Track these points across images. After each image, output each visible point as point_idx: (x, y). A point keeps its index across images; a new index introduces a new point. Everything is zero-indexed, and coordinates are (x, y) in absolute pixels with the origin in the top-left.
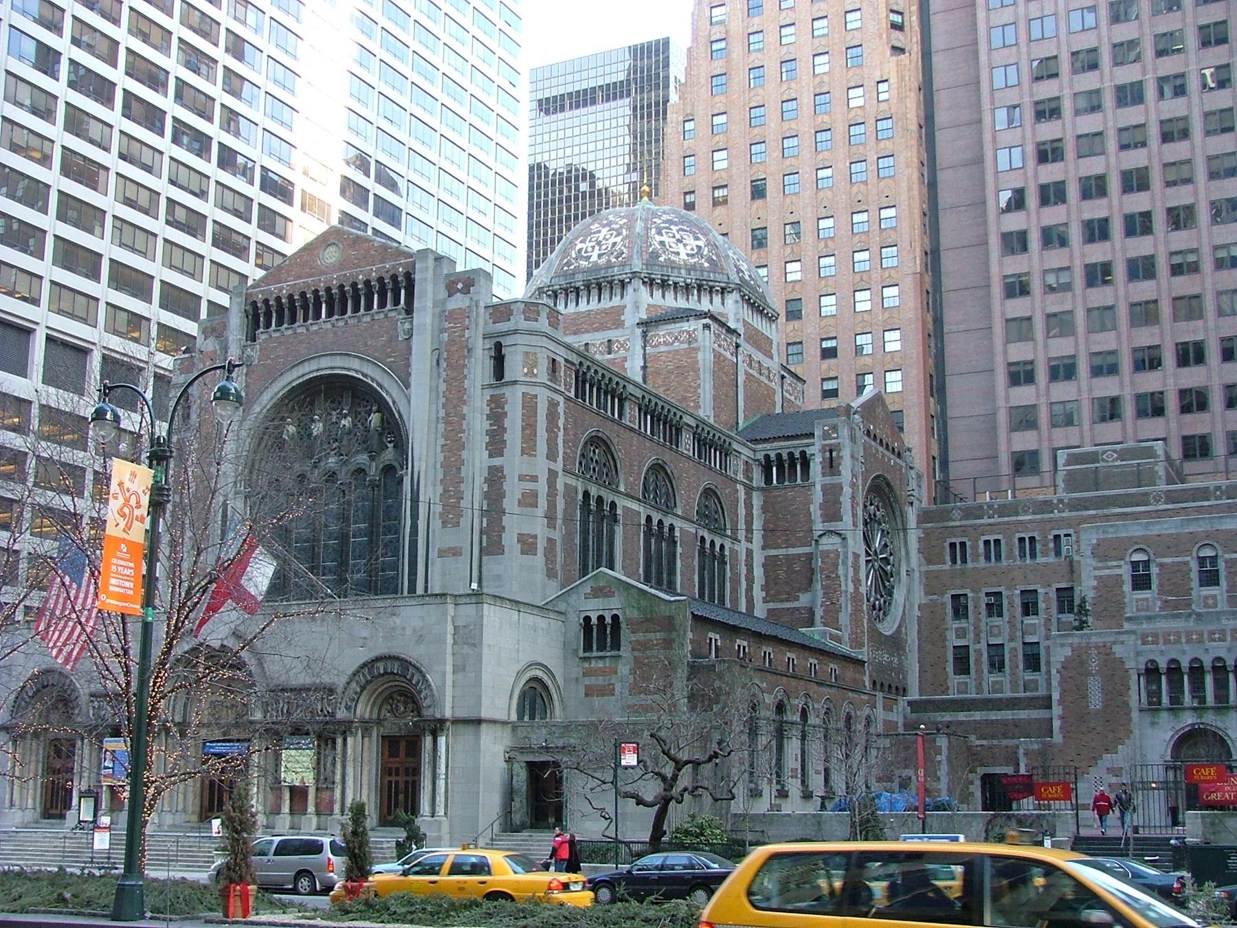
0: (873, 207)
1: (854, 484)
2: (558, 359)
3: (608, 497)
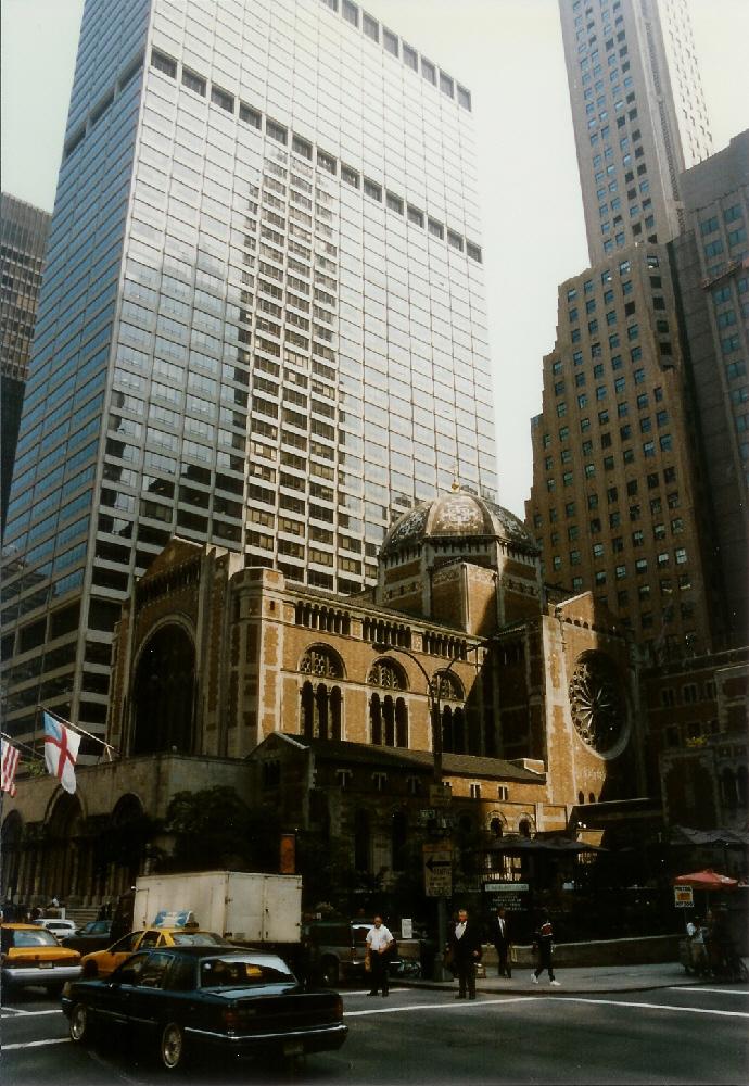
1: (554, 659)
2: (276, 601)
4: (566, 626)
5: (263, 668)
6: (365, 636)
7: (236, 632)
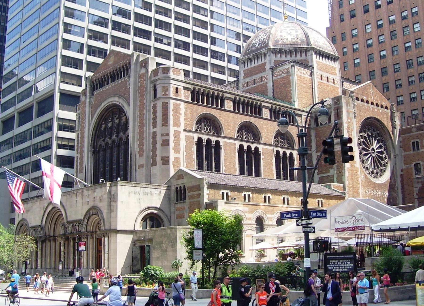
0: (409, 9)
2: (179, 87)
3: (214, 139)
4: (356, 102)
5: (172, 129)
6: (234, 109)
7: (155, 107)
